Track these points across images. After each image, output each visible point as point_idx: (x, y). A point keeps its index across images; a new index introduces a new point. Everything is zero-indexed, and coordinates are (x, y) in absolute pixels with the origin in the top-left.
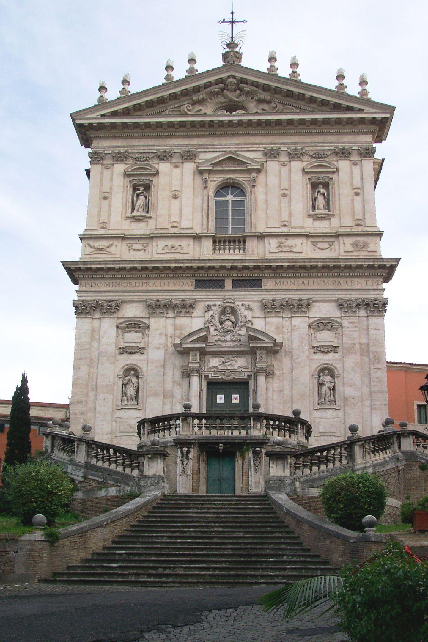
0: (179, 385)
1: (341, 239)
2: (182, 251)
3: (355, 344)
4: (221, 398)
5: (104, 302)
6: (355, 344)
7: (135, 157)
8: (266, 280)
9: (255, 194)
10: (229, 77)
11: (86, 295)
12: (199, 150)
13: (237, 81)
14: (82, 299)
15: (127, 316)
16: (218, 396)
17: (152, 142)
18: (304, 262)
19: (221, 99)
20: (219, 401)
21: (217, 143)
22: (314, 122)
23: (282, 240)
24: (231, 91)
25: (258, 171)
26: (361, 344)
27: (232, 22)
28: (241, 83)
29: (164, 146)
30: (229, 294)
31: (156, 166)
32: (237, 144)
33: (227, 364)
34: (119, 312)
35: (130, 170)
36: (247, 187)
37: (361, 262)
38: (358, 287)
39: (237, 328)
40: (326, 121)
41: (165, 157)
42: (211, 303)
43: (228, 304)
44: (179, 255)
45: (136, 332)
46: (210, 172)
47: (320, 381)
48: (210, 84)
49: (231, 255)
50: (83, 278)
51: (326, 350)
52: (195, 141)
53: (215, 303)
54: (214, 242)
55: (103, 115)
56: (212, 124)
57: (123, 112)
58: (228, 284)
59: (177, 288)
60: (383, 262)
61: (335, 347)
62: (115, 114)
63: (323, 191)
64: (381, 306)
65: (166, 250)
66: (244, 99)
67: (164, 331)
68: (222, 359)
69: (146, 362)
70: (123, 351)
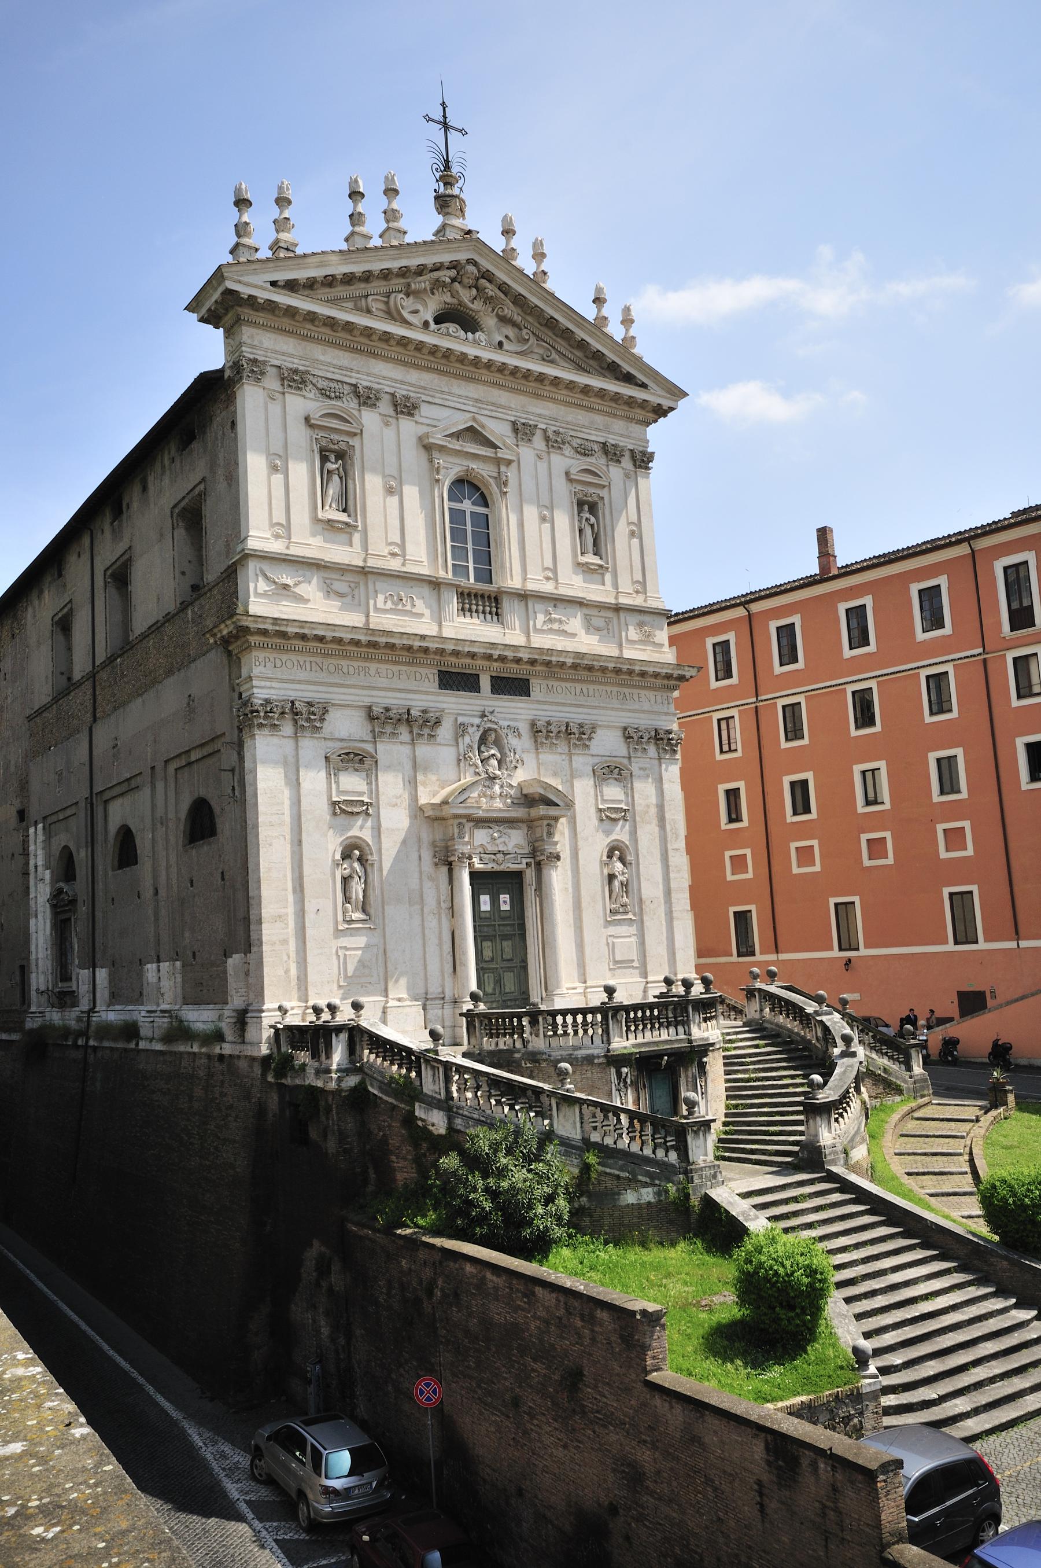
0: (431, 878)
1: (622, 615)
3: (648, 806)
6: (648, 806)
7: (319, 386)
10: (468, 261)
11: (268, 684)
12: (424, 398)
15: (337, 736)
17: (344, 358)
22: (586, 390)
24: (464, 287)
27: (445, 125)
28: (483, 277)
29: (368, 375)
30: (485, 699)
32: (477, 400)
33: (498, 842)
34: (326, 724)
40: (602, 394)
41: (367, 398)
46: (442, 448)
48: (437, 268)
52: (414, 376)
55: (274, 284)
58: (485, 683)
62: (291, 286)
63: (593, 520)
66: (479, 308)
68: (491, 831)
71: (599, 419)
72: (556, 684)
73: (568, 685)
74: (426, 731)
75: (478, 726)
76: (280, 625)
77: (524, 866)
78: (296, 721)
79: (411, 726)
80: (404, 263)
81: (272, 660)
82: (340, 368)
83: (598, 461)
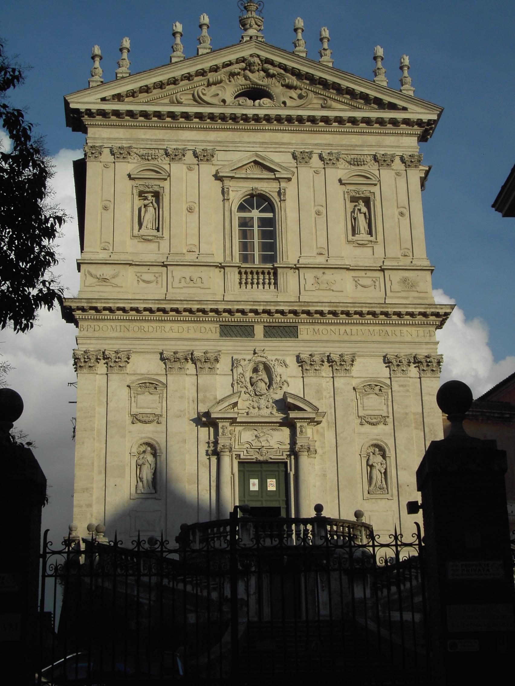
2: (202, 285)
4: (254, 485)
5: (111, 353)
7: (140, 154)
8: (302, 327)
9: (285, 211)
10: (251, 56)
11: (88, 341)
13: (261, 61)
14: (83, 348)
15: (138, 372)
16: (252, 481)
18: (347, 307)
19: (241, 80)
20: (252, 488)
21: (239, 140)
23: (319, 273)
25: (289, 179)
26: (415, 414)
28: (266, 63)
29: (176, 141)
31: (167, 167)
32: (263, 143)
36: (275, 198)
37: (412, 308)
38: (408, 339)
39: (271, 390)
42: (239, 357)
43: (260, 359)
44: (199, 291)
45: (151, 394)
47: (370, 463)
48: (230, 64)
49: (261, 295)
51: (374, 420)
52: (213, 136)
53: (245, 357)
54: (240, 273)
55: (103, 99)
56: (234, 118)
57: (127, 95)
58: (259, 330)
59: (198, 335)
60: (436, 308)
61: (385, 417)
64: (435, 364)
65: (183, 284)
67: (185, 391)
68: (256, 433)
71: (371, 139)
72: (321, 328)
73: (333, 328)
74: (207, 365)
76: (91, 303)
77: (285, 457)
79: (195, 364)
80: (199, 67)
82: (156, 140)
83: (372, 168)
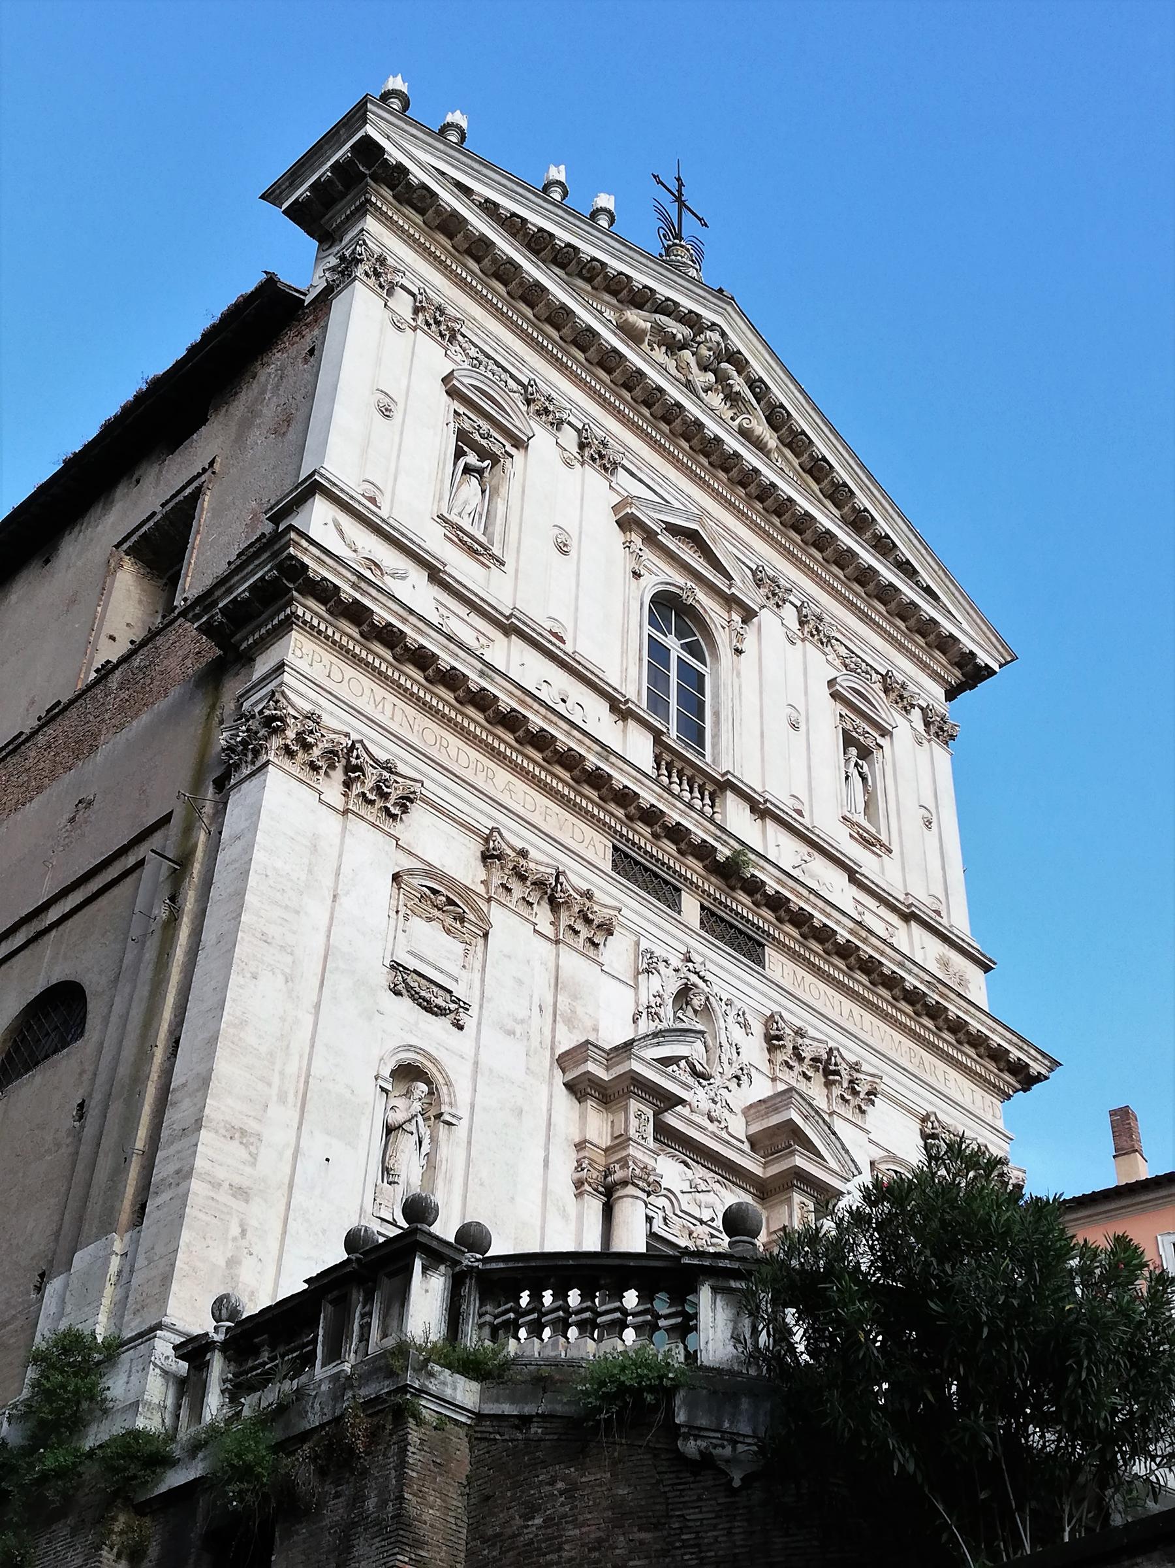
10: (713, 326)
13: (727, 349)
23: (805, 849)
27: (679, 199)
35: (466, 381)
36: (722, 638)
45: (448, 932)
50: (315, 633)
58: (691, 906)
69: (467, 1068)
70: (409, 984)
75: (676, 970)
78: (347, 784)
81: (326, 661)
